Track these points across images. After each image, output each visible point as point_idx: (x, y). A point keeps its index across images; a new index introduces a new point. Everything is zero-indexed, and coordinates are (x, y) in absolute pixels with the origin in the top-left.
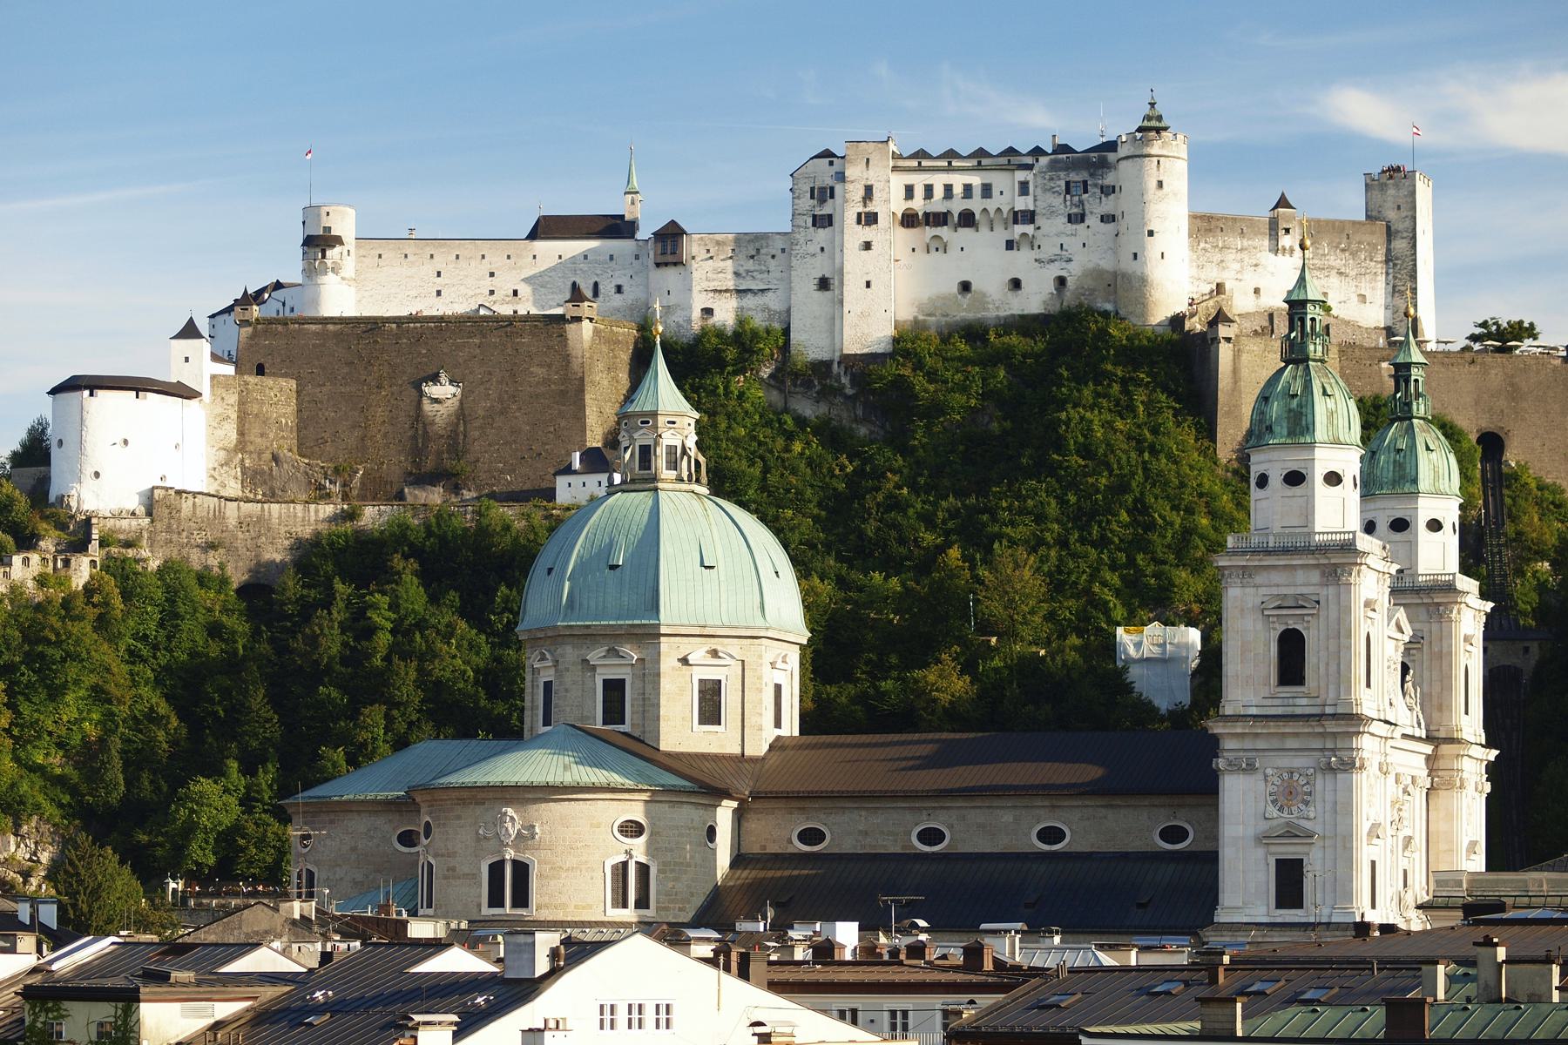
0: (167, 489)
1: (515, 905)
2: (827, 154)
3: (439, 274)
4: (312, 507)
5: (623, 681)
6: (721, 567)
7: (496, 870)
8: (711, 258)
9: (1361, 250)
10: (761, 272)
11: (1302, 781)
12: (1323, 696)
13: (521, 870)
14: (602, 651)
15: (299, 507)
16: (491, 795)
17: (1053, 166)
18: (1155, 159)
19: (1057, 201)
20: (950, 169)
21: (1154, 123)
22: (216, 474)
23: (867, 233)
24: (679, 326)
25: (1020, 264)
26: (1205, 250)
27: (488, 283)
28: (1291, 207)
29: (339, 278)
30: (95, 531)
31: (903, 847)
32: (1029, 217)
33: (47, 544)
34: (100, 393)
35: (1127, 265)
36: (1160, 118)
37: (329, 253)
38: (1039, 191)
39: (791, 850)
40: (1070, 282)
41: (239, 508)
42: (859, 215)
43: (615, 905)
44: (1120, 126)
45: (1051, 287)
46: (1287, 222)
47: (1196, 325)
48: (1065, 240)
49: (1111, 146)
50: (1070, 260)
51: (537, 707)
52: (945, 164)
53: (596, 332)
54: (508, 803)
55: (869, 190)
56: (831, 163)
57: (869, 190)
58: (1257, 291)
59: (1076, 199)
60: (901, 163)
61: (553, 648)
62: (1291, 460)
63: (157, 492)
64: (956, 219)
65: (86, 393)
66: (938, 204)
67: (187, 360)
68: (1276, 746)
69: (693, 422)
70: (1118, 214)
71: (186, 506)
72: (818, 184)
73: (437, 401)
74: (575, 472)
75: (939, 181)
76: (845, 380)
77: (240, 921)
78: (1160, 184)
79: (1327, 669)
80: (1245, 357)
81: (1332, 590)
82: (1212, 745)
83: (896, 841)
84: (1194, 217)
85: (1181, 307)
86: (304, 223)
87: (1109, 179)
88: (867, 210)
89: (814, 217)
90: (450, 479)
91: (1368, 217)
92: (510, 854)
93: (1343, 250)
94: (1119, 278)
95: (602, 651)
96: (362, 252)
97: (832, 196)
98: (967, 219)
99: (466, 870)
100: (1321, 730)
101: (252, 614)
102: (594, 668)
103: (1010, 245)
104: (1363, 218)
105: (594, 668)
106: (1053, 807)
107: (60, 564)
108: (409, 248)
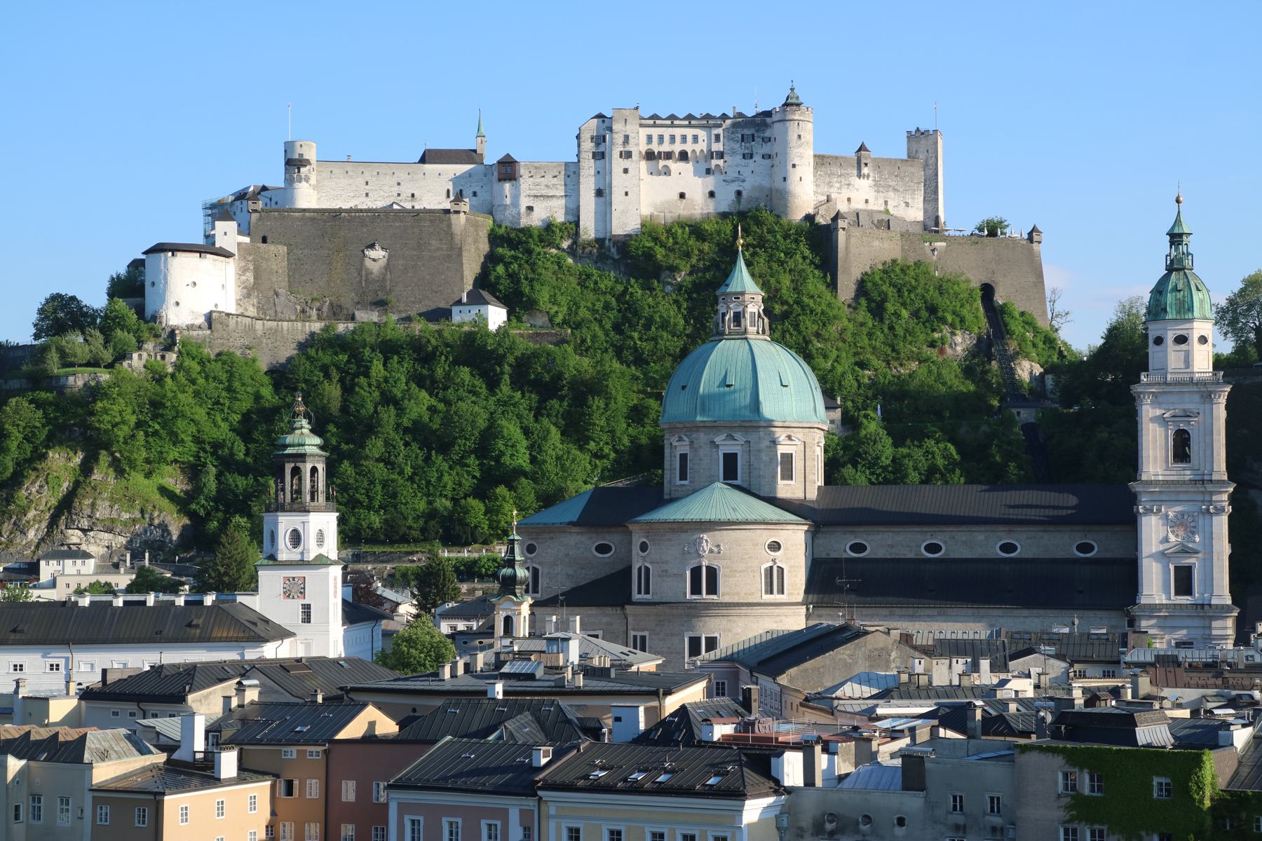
0: (220, 312)
1: (708, 593)
2: (600, 116)
3: (367, 183)
4: (307, 324)
5: (736, 455)
6: (791, 385)
7: (696, 572)
8: (532, 176)
9: (906, 176)
11: (1190, 519)
12: (1202, 469)
13: (712, 573)
14: (723, 436)
15: (299, 324)
16: (693, 527)
17: (734, 125)
18: (797, 122)
19: (737, 146)
20: (672, 126)
21: (794, 101)
22: (241, 303)
23: (626, 163)
24: (513, 217)
26: (820, 175)
27: (396, 189)
28: (868, 151)
29: (308, 185)
30: (178, 338)
31: (916, 554)
32: (721, 155)
33: (149, 346)
34: (179, 254)
35: (778, 184)
36: (797, 98)
37: (302, 170)
38: (726, 140)
39: (845, 556)
40: (744, 194)
41: (263, 324)
42: (621, 152)
43: (766, 593)
44: (773, 102)
45: (733, 196)
46: (866, 159)
47: (820, 220)
49: (768, 114)
50: (744, 181)
51: (675, 469)
52: (687, 122)
53: (467, 220)
54: (704, 531)
55: (627, 138)
56: (603, 121)
57: (627, 138)
58: (849, 200)
59: (748, 144)
60: (644, 122)
61: (688, 434)
62: (1180, 330)
63: (214, 314)
64: (677, 156)
65: (170, 254)
66: (666, 147)
67: (225, 234)
68: (1175, 498)
69: (760, 297)
70: (773, 154)
71: (232, 322)
73: (374, 260)
74: (464, 304)
75: (667, 132)
76: (613, 250)
77: (865, 642)
78: (799, 137)
79: (1205, 453)
80: (853, 240)
81: (1207, 406)
82: (1133, 499)
83: (911, 551)
84: (815, 156)
85: (811, 211)
86: (285, 151)
87: (767, 134)
88: (626, 149)
90: (381, 304)
91: (909, 157)
92: (705, 563)
93: (896, 176)
94: (774, 193)
95: (723, 436)
96: (320, 169)
98: (684, 156)
99: (676, 572)
100: (1202, 489)
101: (277, 386)
102: (718, 446)
103: (708, 171)
104: (905, 157)
105: (718, 446)
106: (1010, 531)
107: (159, 358)
108: (349, 167)
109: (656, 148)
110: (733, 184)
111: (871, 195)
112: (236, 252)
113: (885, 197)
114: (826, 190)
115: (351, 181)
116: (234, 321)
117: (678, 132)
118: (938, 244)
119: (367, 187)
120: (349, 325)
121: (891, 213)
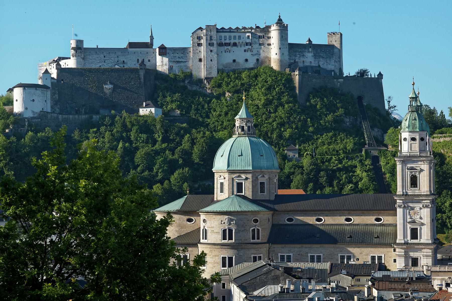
0: (44, 112)
3: (105, 57)
4: (80, 116)
9: (327, 52)
10: (185, 57)
15: (77, 116)
20: (230, 32)
22: (53, 107)
23: (212, 48)
25: (248, 55)
26: (291, 52)
32: (251, 44)
41: (62, 116)
42: (209, 43)
45: (255, 61)
48: (258, 50)
55: (211, 37)
57: (211, 37)
66: (227, 41)
71: (49, 116)
72: (199, 36)
75: (227, 34)
89: (198, 43)
93: (323, 52)
97: (202, 39)
98: (235, 44)
103: (245, 51)
109: (224, 42)
110: (255, 56)
111: (312, 60)
112: (51, 87)
113: (318, 60)
114: (294, 58)
115: (98, 56)
116: (50, 115)
117: (233, 34)
118: (340, 80)
119: (105, 58)
120: (97, 116)
121: (321, 66)
